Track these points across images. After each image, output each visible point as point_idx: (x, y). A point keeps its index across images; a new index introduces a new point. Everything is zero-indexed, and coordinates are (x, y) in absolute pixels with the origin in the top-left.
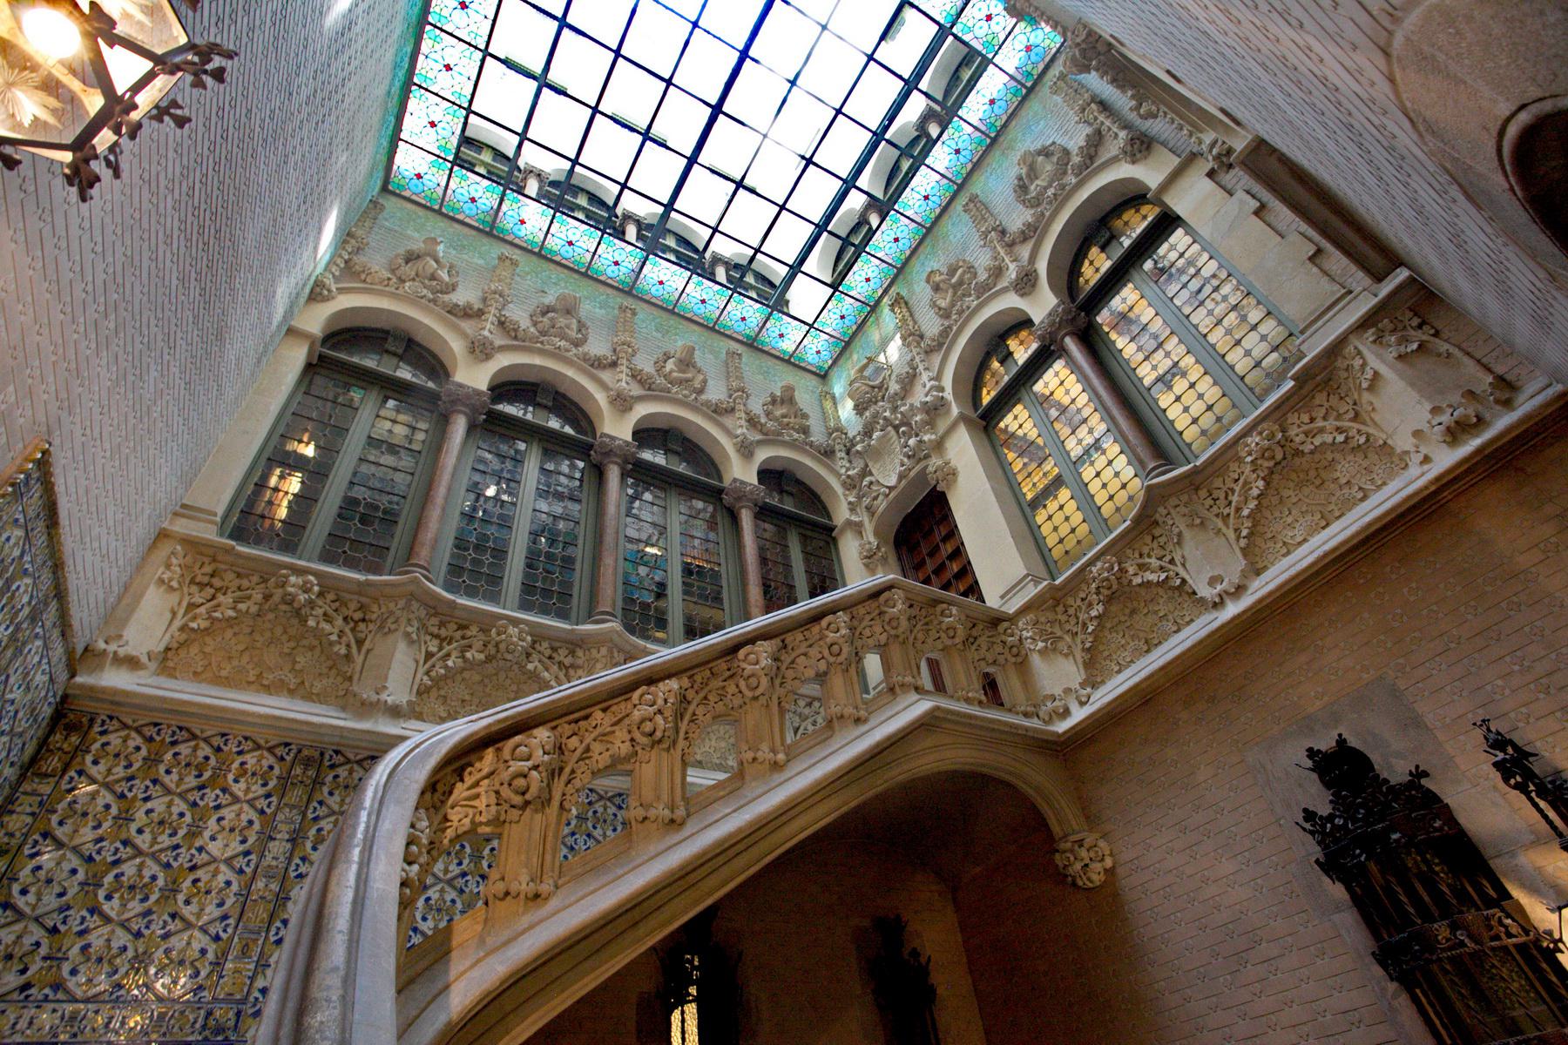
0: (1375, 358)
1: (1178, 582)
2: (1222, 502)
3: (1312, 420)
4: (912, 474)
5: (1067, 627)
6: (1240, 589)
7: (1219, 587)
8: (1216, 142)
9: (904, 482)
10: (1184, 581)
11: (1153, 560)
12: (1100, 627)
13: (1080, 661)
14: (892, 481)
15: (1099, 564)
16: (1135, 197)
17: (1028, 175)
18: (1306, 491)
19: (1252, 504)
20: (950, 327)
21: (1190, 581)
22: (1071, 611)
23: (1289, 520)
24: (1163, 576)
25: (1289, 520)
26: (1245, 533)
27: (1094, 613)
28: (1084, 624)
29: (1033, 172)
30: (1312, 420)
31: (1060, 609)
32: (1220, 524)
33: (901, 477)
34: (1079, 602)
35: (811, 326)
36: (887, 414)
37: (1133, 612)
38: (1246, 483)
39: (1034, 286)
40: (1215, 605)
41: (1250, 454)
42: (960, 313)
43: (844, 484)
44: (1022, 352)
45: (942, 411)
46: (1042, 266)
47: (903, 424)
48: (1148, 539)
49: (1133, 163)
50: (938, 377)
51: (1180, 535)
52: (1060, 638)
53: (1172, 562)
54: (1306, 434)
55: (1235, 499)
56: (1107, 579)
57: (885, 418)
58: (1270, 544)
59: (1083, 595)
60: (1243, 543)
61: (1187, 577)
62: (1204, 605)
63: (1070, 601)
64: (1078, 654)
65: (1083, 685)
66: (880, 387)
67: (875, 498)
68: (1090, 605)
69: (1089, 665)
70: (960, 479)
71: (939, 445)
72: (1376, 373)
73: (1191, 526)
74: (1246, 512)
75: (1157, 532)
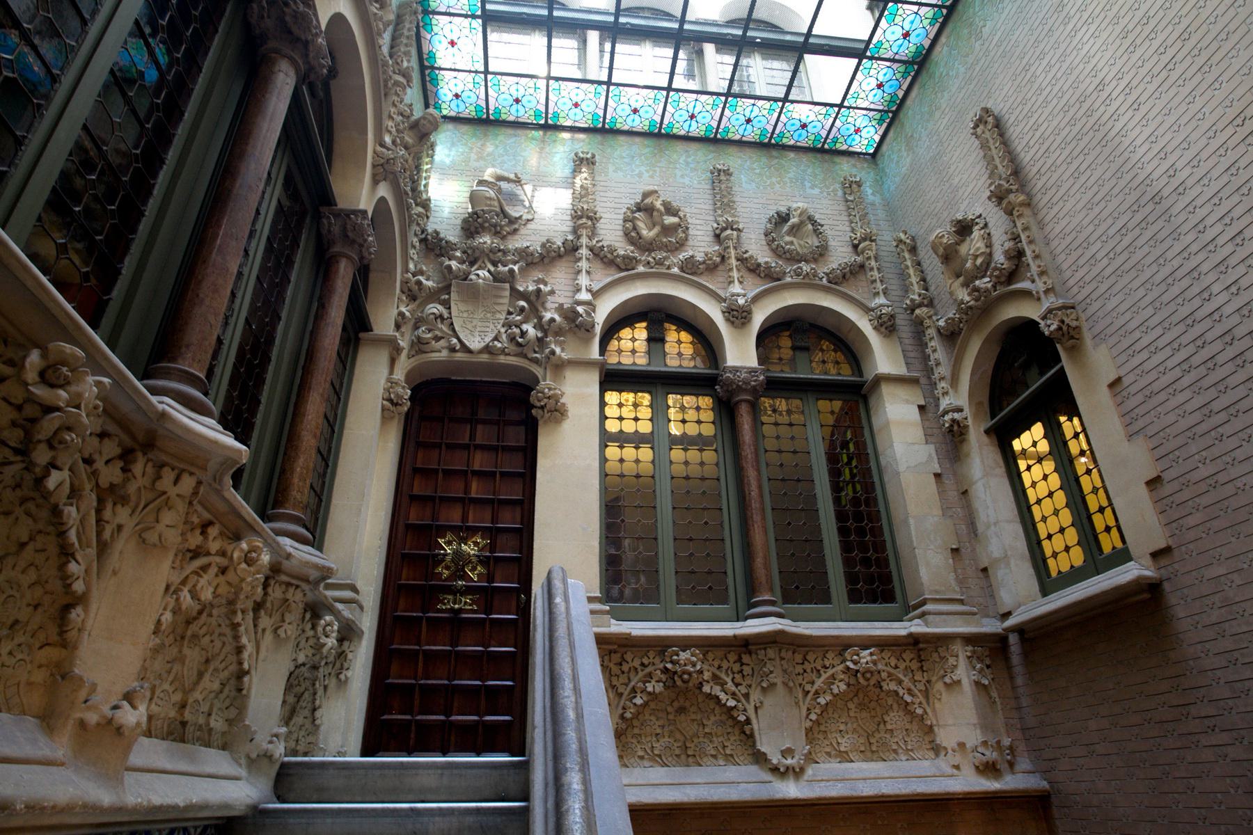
0: (963, 670)
1: (742, 718)
2: (808, 677)
3: (896, 667)
4: (502, 359)
6: (796, 773)
7: (789, 762)
8: (960, 410)
9: (484, 358)
10: (748, 721)
11: (729, 680)
12: (646, 704)
14: (475, 343)
16: (845, 343)
17: (793, 227)
18: (864, 714)
19: (829, 698)
20: (638, 262)
21: (755, 727)
22: (625, 667)
23: (842, 727)
24: (731, 703)
25: (842, 727)
26: (813, 717)
29: (795, 230)
30: (896, 667)
31: (616, 658)
32: (800, 696)
33: (487, 349)
34: (637, 663)
35: (486, 72)
36: (516, 268)
37: (682, 710)
38: (833, 677)
39: (743, 324)
40: (775, 770)
41: (855, 663)
42: (660, 263)
43: (405, 282)
44: (680, 351)
45: (582, 333)
46: (759, 317)
47: (524, 296)
48: (732, 657)
49: (875, 328)
50: (596, 294)
51: (773, 685)
53: (747, 696)
54: (890, 675)
55: (819, 683)
56: (690, 674)
57: (512, 271)
58: (821, 736)
59: (646, 661)
60: (809, 724)
61: (754, 721)
62: (760, 758)
63: (628, 657)
66: (513, 221)
67: (437, 339)
70: (567, 425)
71: (559, 367)
72: (959, 682)
73: (786, 684)
74: (822, 701)
75: (746, 658)
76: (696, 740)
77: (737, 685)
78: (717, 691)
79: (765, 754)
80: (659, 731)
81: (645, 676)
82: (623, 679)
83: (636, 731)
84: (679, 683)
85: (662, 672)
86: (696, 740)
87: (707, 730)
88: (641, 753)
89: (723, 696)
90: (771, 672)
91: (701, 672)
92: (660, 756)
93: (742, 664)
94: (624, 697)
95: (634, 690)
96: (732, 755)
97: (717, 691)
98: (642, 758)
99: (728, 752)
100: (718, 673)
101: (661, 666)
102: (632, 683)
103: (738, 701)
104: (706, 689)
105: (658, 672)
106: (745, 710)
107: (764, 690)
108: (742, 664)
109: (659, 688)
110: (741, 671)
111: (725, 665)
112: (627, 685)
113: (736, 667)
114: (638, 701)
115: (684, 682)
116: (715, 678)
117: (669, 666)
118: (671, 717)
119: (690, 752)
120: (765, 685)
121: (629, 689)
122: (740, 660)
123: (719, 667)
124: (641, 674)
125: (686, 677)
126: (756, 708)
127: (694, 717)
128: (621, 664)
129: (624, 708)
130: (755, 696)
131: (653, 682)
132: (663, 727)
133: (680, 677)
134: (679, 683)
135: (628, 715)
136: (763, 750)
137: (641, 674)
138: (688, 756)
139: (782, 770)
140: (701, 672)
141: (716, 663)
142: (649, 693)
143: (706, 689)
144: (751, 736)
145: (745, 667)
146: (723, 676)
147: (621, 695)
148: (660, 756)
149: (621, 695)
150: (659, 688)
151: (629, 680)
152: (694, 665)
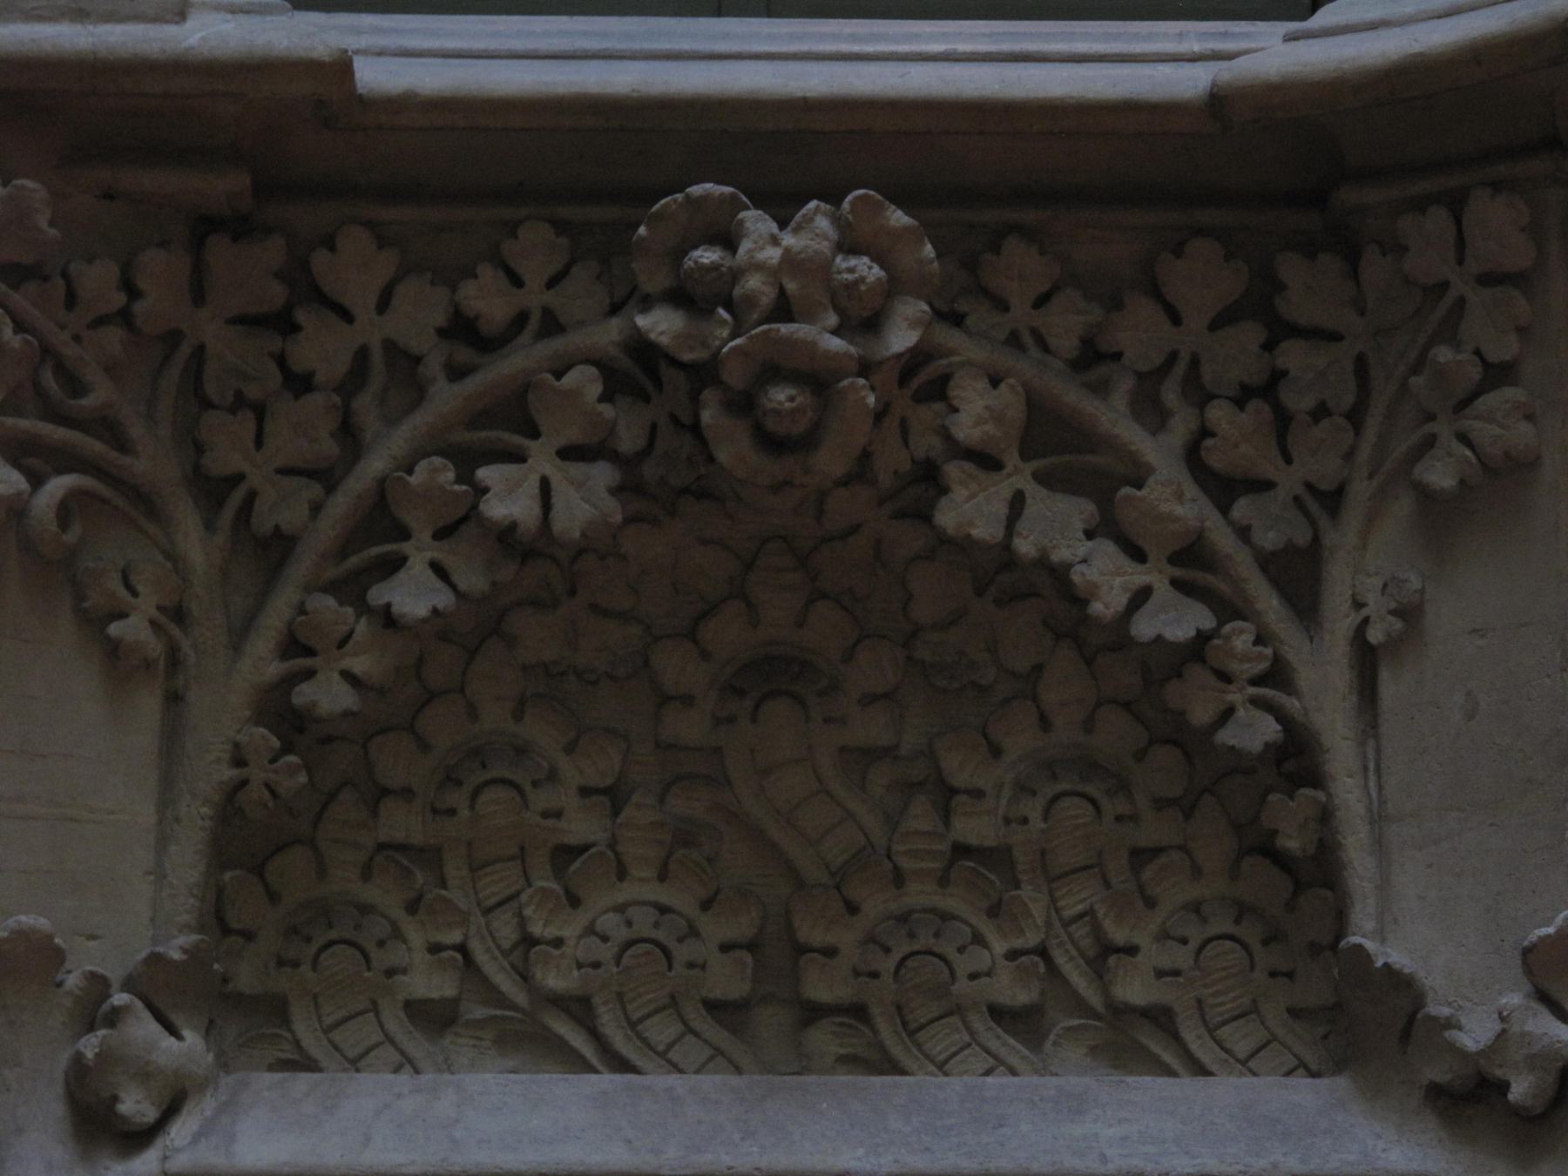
1: (1254, 732)
5: (228, 449)
10: (1296, 758)
11: (1160, 454)
12: (475, 630)
13: (209, 771)
15: (816, 228)
21: (1348, 791)
22: (322, 348)
24: (1174, 621)
27: (508, 498)
28: (381, 521)
31: (250, 273)
34: (417, 318)
37: (772, 677)
48: (1204, 278)
52: (144, 501)
53: (1297, 574)
56: (819, 380)
59: (487, 299)
63: (354, 267)
64: (223, 712)
65: (160, 988)
68: (510, 421)
69: (245, 841)
75: (1308, 289)
76: (876, 904)
77: (1224, 489)
78: (1056, 528)
79: (1399, 983)
80: (582, 826)
81: (480, 418)
82: (303, 429)
83: (401, 823)
84: (733, 448)
85: (615, 385)
86: (876, 904)
87: (973, 828)
88: (430, 982)
89: (1107, 577)
90: (1497, 374)
91: (925, 379)
92: (579, 1008)
93: (1280, 331)
94: (300, 568)
95: (381, 521)
96: (1160, 1018)
97: (1056, 528)
98: (435, 1019)
99: (1134, 989)
100: (1071, 395)
101: (608, 335)
102: (375, 464)
103: (1229, 609)
104: (971, 509)
105: (585, 381)
106: (1277, 675)
107: (1440, 520)
108: (1280, 331)
109: (584, 500)
110: (1268, 388)
111: (1140, 335)
112: (327, 477)
113: (1237, 355)
114: (413, 595)
115: (772, 443)
116: (1057, 447)
117: (661, 324)
118: (688, 727)
119: (821, 987)
120: (1440, 475)
121: (341, 504)
122: (1259, 305)
123: (1092, 357)
124: (445, 398)
125: (780, 396)
126: (1367, 661)
127: (872, 729)
128: (283, 323)
129: (294, 646)
130: (1367, 567)
131: (542, 460)
132: (614, 796)
133: (744, 404)
134: (733, 448)
135: (327, 695)
136: (1393, 954)
137: (445, 398)
138: (813, 1013)
139: (1520, 1089)
140: (925, 379)
141: (1066, 324)
142: (506, 534)
143: (971, 509)
144: (1318, 874)
145: (1292, 355)
146: (1113, 417)
147: (276, 550)
148: (579, 1008)
149: (276, 550)
150: (584, 500)
151: (349, 433)
152: (865, 322)
